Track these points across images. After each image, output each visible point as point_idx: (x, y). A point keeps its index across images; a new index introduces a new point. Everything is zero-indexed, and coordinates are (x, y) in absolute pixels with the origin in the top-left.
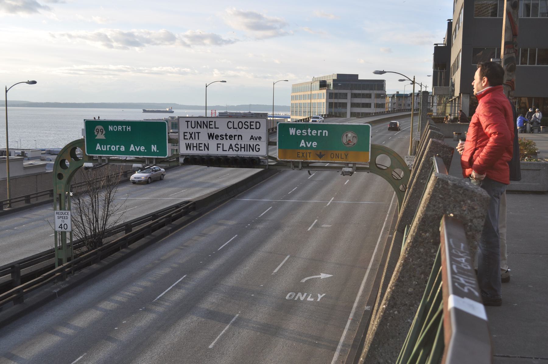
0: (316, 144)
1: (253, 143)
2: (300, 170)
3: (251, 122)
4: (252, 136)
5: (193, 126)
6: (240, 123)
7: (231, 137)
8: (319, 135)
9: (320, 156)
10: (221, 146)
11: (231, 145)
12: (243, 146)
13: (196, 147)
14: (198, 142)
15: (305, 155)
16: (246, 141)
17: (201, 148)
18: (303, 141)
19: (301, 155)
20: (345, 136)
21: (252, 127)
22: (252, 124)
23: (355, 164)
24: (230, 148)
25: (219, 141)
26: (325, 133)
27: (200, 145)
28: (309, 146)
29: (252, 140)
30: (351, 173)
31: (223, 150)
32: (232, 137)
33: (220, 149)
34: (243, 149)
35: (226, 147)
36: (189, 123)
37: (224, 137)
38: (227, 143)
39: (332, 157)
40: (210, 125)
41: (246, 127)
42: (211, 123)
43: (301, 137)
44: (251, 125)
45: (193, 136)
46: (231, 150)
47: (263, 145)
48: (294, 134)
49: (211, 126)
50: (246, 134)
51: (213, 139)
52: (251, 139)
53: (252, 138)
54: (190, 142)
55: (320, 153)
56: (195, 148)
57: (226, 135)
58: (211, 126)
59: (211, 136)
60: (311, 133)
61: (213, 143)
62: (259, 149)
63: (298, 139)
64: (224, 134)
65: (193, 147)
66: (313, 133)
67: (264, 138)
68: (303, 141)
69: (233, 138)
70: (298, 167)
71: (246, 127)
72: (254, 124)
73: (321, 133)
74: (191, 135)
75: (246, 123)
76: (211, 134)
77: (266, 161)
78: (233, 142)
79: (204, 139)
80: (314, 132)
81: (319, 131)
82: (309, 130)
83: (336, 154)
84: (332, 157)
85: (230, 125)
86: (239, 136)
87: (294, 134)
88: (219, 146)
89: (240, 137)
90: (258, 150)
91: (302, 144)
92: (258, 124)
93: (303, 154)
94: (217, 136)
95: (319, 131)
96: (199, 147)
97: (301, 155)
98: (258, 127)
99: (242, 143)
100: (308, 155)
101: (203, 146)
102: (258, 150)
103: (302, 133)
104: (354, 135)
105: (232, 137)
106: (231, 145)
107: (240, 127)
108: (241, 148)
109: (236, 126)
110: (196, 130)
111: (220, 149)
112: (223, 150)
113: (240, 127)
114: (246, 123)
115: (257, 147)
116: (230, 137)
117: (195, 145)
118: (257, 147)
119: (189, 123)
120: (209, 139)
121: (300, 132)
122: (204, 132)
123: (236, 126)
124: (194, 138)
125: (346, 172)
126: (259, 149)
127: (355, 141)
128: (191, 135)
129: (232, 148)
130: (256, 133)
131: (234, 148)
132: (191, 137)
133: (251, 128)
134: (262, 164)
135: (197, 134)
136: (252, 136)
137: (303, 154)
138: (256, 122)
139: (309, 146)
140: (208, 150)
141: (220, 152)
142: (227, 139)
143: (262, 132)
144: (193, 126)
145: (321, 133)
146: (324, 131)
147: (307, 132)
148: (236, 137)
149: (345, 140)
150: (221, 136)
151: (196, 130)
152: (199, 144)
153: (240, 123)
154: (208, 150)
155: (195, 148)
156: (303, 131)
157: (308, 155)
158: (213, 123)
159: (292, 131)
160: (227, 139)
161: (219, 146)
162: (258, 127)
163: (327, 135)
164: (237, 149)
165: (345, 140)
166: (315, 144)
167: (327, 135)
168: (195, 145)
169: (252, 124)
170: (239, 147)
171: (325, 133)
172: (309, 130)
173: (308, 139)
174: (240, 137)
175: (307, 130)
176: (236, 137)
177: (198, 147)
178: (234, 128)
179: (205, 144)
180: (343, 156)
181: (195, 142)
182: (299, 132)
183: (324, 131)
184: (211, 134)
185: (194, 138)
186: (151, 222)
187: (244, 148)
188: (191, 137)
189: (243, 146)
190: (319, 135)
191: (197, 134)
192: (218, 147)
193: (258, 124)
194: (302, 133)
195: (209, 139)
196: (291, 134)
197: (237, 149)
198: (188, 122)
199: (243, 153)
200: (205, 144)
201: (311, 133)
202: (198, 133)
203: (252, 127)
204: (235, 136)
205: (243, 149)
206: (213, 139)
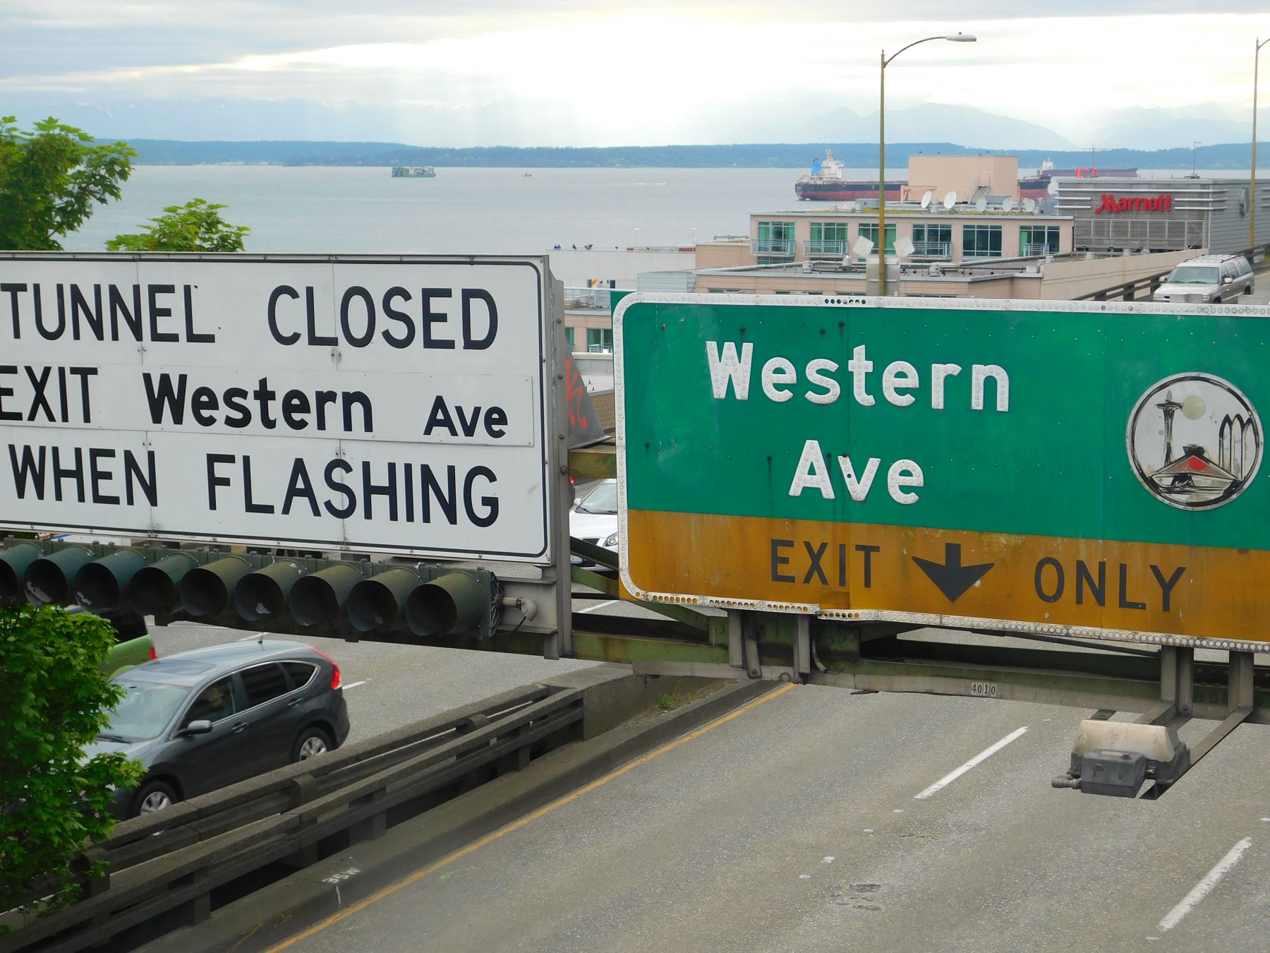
0: (917, 479)
1: (448, 454)
2: (805, 679)
3: (428, 294)
4: (439, 403)
5: (51, 324)
6: (357, 303)
7: (295, 403)
8: (938, 401)
9: (952, 579)
10: (233, 472)
11: (299, 467)
12: (380, 478)
13: (77, 474)
14: (88, 442)
15: (828, 563)
16: (399, 439)
17: (105, 488)
18: (812, 451)
19: (799, 562)
20: (1151, 417)
21: (438, 332)
22: (437, 305)
23: (1249, 655)
24: (292, 492)
25: (221, 438)
26: (990, 383)
27: (103, 464)
28: (859, 489)
29: (441, 432)
30: (1159, 776)
31: (251, 507)
32: (304, 408)
33: (230, 497)
34: (380, 503)
35: (270, 488)
36: (26, 299)
37: (253, 405)
38: (272, 452)
39: (1049, 588)
40: (156, 313)
41: (400, 331)
42: (162, 301)
43: (800, 418)
44: (429, 318)
45: (52, 392)
46: (300, 503)
47: (519, 469)
48: (742, 392)
49: (164, 325)
50: (402, 382)
51: (178, 419)
52: (432, 423)
53: (439, 416)
54: (36, 435)
55: (953, 551)
56: (69, 484)
57: (264, 395)
58: (164, 325)
59: (165, 398)
60: (874, 382)
61: (181, 448)
62: (491, 502)
63: (766, 432)
64: (252, 387)
65: (59, 474)
66: (889, 381)
67: (525, 423)
68: (812, 451)
69: (311, 418)
70: (785, 655)
71: (400, 331)
72: (450, 307)
73: (959, 386)
74: (39, 386)
75: (397, 304)
76: (165, 379)
77: (548, 602)
78: (315, 448)
79: (120, 418)
80: (899, 379)
81: (940, 372)
82: (860, 364)
83: (1081, 568)
84: (1049, 588)
85: (291, 316)
86: (349, 399)
87: (742, 392)
88: (221, 470)
89: (357, 409)
90: (483, 512)
91: (810, 471)
92: (478, 306)
93: (816, 557)
94: (204, 399)
95: (940, 372)
96: (98, 475)
97: (799, 562)
98: (479, 333)
99: (375, 452)
100: (856, 561)
101: (115, 466)
102: (483, 512)
103: (802, 385)
104: (1233, 407)
105: (304, 408)
106: (299, 467)
107: (359, 331)
108: (369, 490)
109: (328, 325)
110: (67, 352)
111: (230, 497)
112: (251, 507)
113: (359, 331)
114: (397, 304)
115: (481, 487)
116: (288, 409)
117: (68, 463)
118: (481, 487)
119: (26, 299)
120: (157, 418)
121: (790, 376)
122: (122, 365)
123: (328, 325)
124: (57, 412)
125: (1102, 766)
126: (491, 502)
127: (1246, 455)
128: (39, 386)
129: (308, 492)
130: (466, 380)
131: (323, 492)
132: (40, 400)
133: (429, 343)
134: (513, 620)
135: (74, 382)
136: (439, 403)
137: (816, 557)
138: (468, 295)
139: (859, 489)
140: (154, 502)
141: (230, 521)
142: (269, 424)
143: (507, 375)
144: (51, 324)
145: (959, 386)
146: (980, 373)
147: (844, 377)
148: (334, 411)
149: (1149, 451)
150: (231, 394)
151: (67, 352)
152: (95, 453)
153: (357, 303)
154: (154, 502)
155: (69, 484)
156: (813, 368)
157: (856, 561)
158: (174, 301)
159: (728, 369)
160: (269, 424)
161: (221, 470)
162: (479, 333)
163: (1002, 404)
164: (341, 501)
165: (1149, 451)
166: (905, 478)
167: (1002, 404)
168: (68, 463)
169: (437, 305)
170: (355, 481)
171: (990, 383)
172: (860, 364)
173: (849, 431)
174: (357, 409)
175: (844, 357)
176: (334, 411)
177: (86, 473)
178: (314, 340)
179: (129, 457)
180: (1144, 588)
181: (67, 439)
182: (778, 375)
183: (980, 373)
184: (165, 379)
185: (57, 412)
186: (275, 820)
187: (390, 491)
188: (40, 400)
189: (380, 478)
190: (938, 401)
191: (74, 382)
192: (214, 481)
193: (478, 306)
194: (802, 385)
195: (157, 418)
196: (719, 391)
197: (341, 501)
198: (15, 289)
199: (381, 533)
200: (129, 457)
201: (874, 382)
202: (85, 373)
203: (438, 332)
204: (325, 397)
205: (380, 503)
206: (178, 419)
